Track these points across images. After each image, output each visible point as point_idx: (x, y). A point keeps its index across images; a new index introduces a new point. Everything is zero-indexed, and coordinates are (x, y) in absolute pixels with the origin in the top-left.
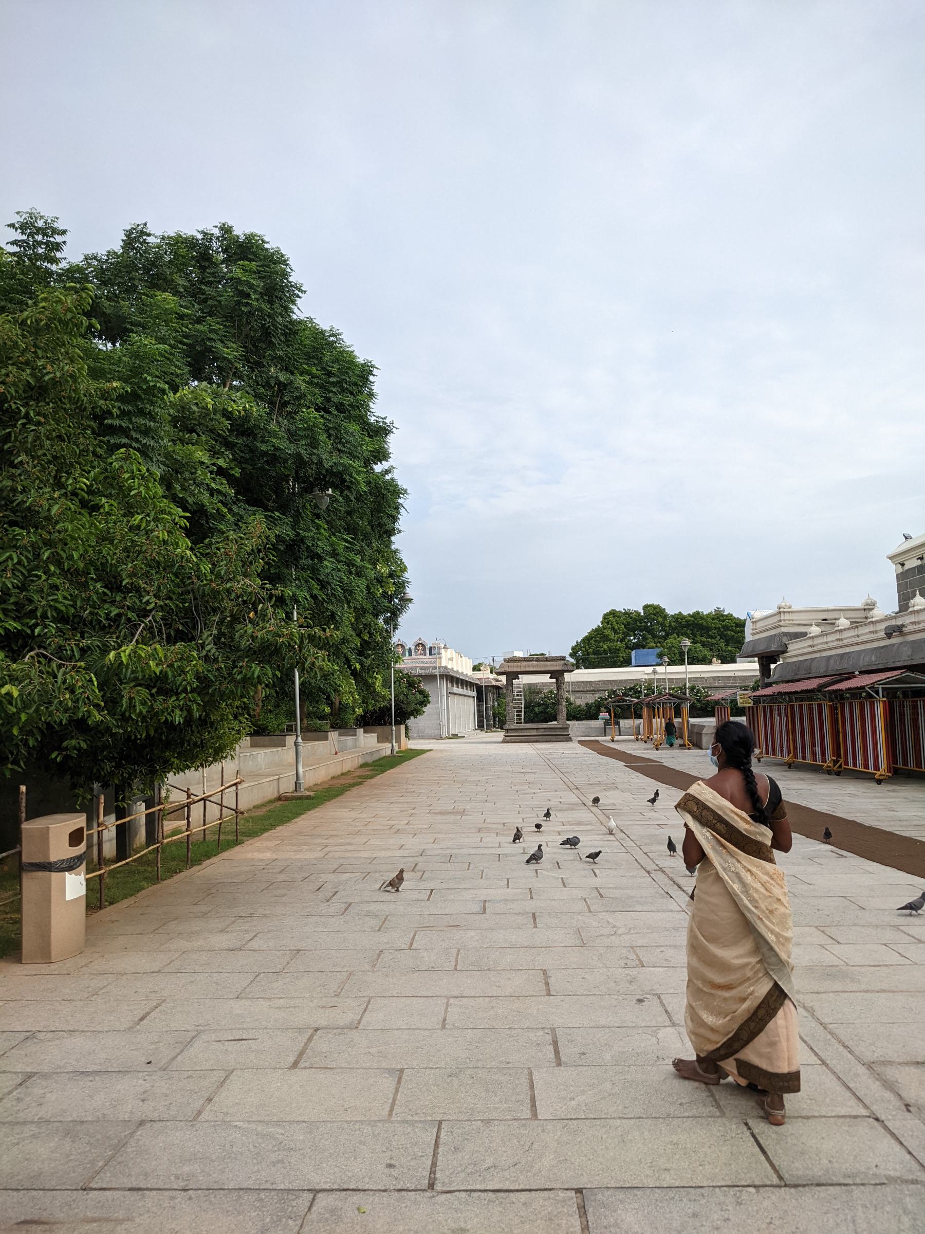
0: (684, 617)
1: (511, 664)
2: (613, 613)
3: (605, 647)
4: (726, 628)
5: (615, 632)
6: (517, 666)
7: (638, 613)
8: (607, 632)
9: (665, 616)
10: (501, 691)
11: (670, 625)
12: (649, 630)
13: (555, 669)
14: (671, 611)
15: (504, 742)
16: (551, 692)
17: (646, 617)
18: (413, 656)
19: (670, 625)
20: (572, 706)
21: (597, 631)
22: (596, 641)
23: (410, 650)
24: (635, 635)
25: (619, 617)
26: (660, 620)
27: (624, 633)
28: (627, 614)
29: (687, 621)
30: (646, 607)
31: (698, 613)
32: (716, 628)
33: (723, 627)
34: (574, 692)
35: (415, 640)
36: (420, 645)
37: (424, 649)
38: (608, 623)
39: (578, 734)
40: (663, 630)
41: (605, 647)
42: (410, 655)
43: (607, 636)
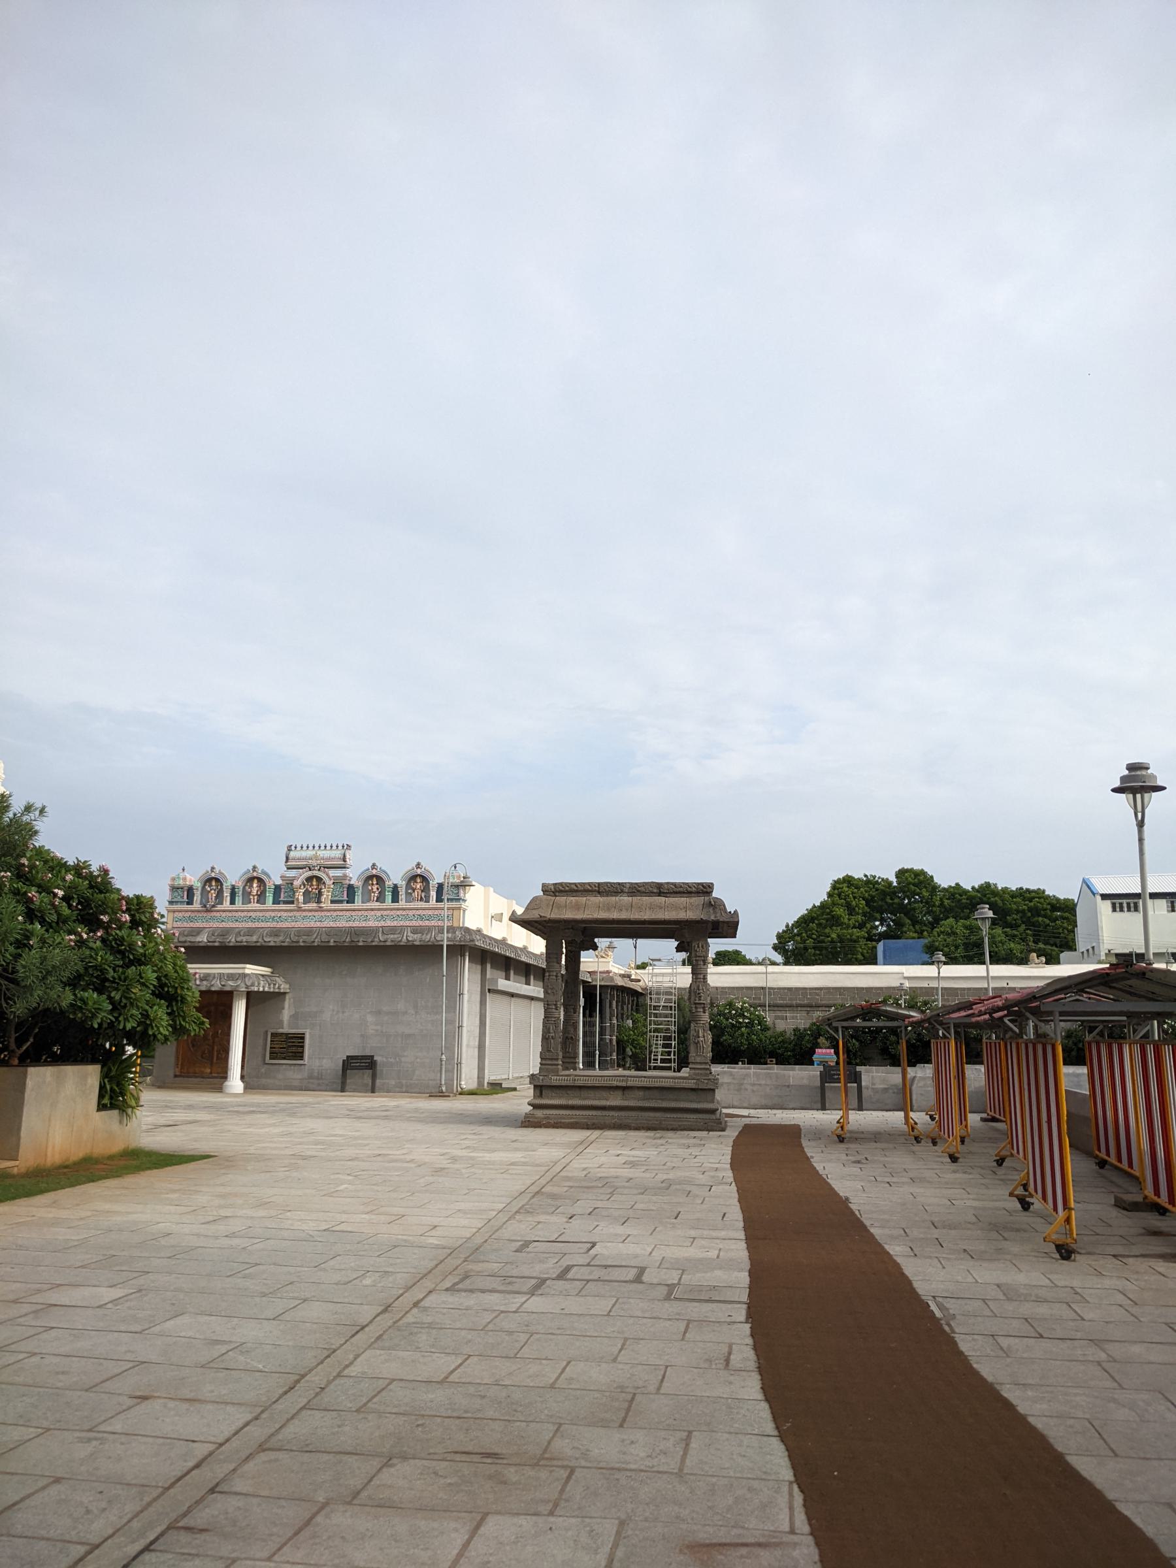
0: (966, 892)
1: (561, 899)
2: (848, 881)
3: (834, 936)
4: (1036, 912)
5: (851, 910)
6: (577, 907)
7: (890, 884)
8: (839, 911)
9: (934, 888)
10: (641, 999)
11: (942, 904)
12: (907, 911)
13: (682, 915)
14: (944, 880)
15: (528, 1122)
16: (731, 1005)
17: (901, 889)
18: (402, 903)
19: (942, 904)
20: (769, 1033)
21: (823, 906)
22: (820, 925)
23: (395, 890)
24: (882, 921)
25: (858, 888)
26: (926, 894)
27: (864, 914)
28: (870, 882)
29: (971, 898)
30: (901, 873)
31: (988, 885)
32: (1018, 911)
33: (1030, 909)
34: (774, 1007)
35: (408, 866)
36: (418, 879)
37: (426, 889)
38: (839, 895)
39: (755, 1100)
40: (929, 913)
41: (834, 936)
42: (395, 899)
43: (839, 917)
